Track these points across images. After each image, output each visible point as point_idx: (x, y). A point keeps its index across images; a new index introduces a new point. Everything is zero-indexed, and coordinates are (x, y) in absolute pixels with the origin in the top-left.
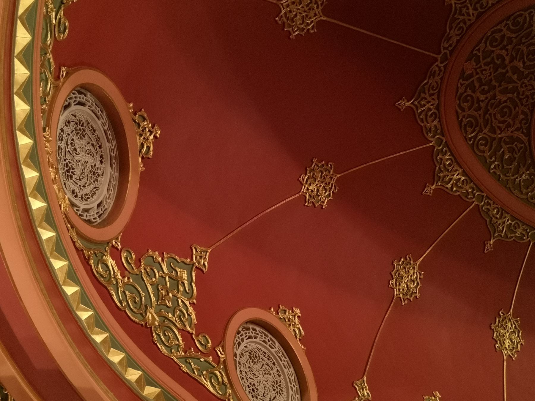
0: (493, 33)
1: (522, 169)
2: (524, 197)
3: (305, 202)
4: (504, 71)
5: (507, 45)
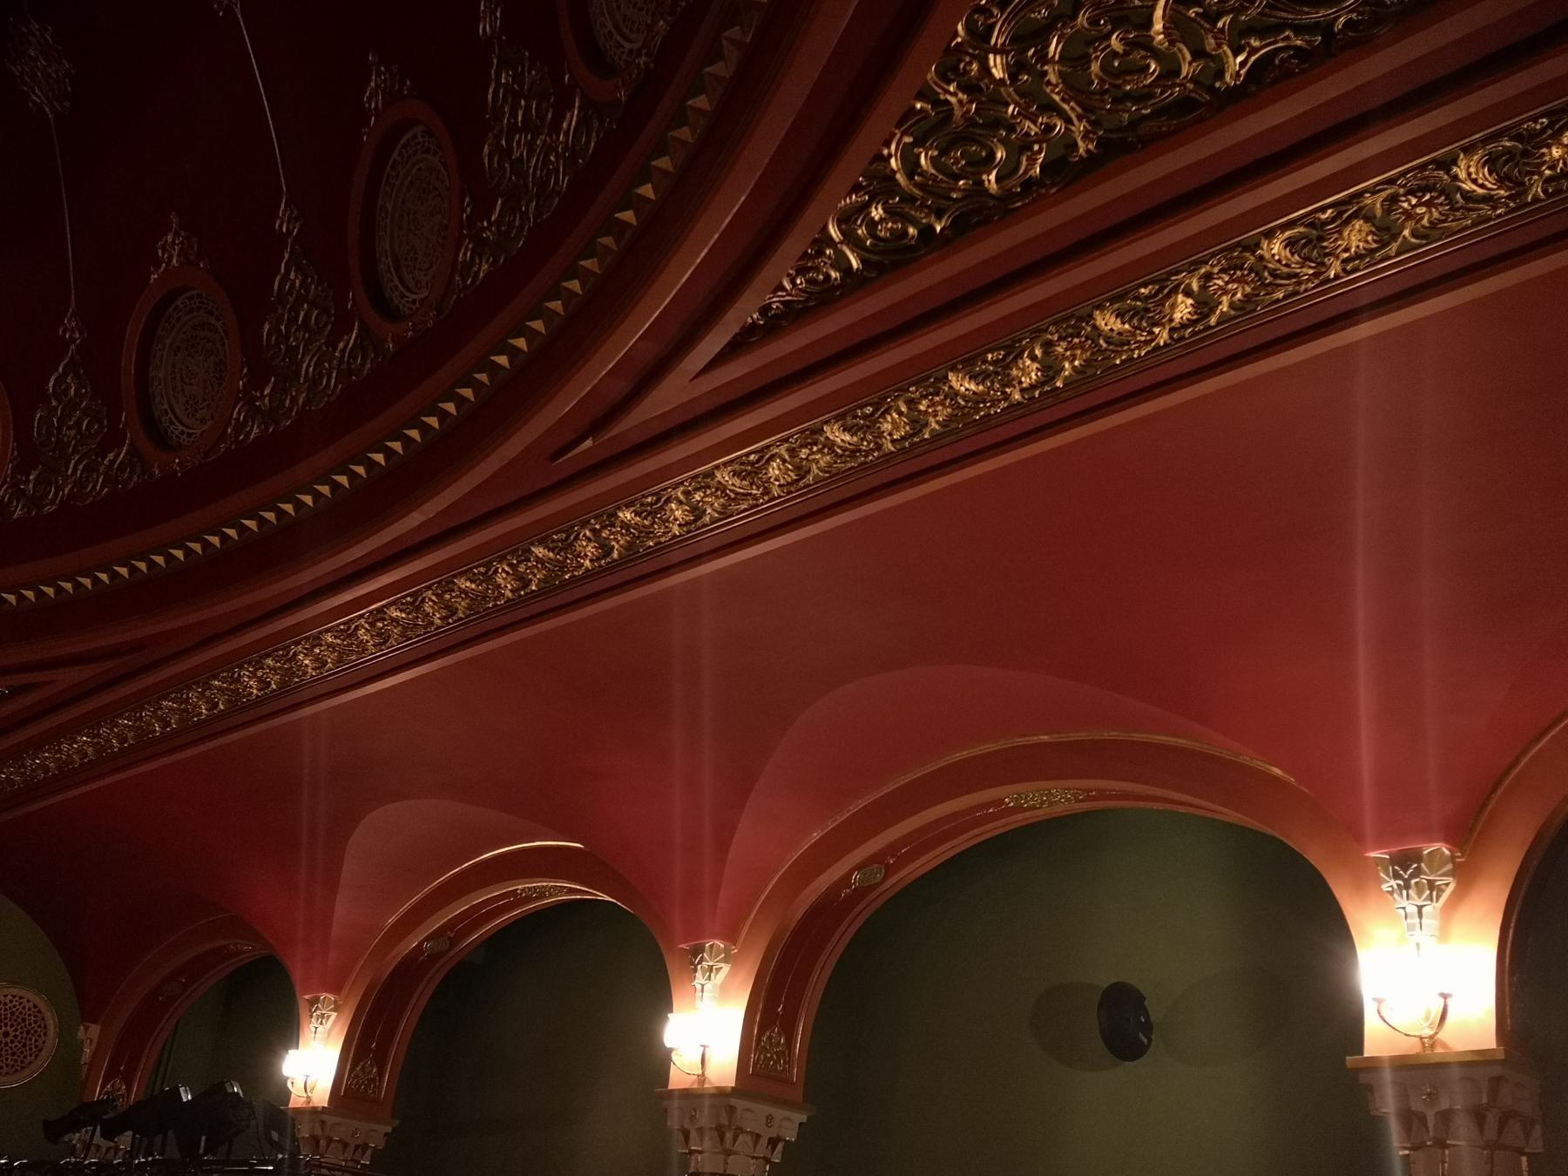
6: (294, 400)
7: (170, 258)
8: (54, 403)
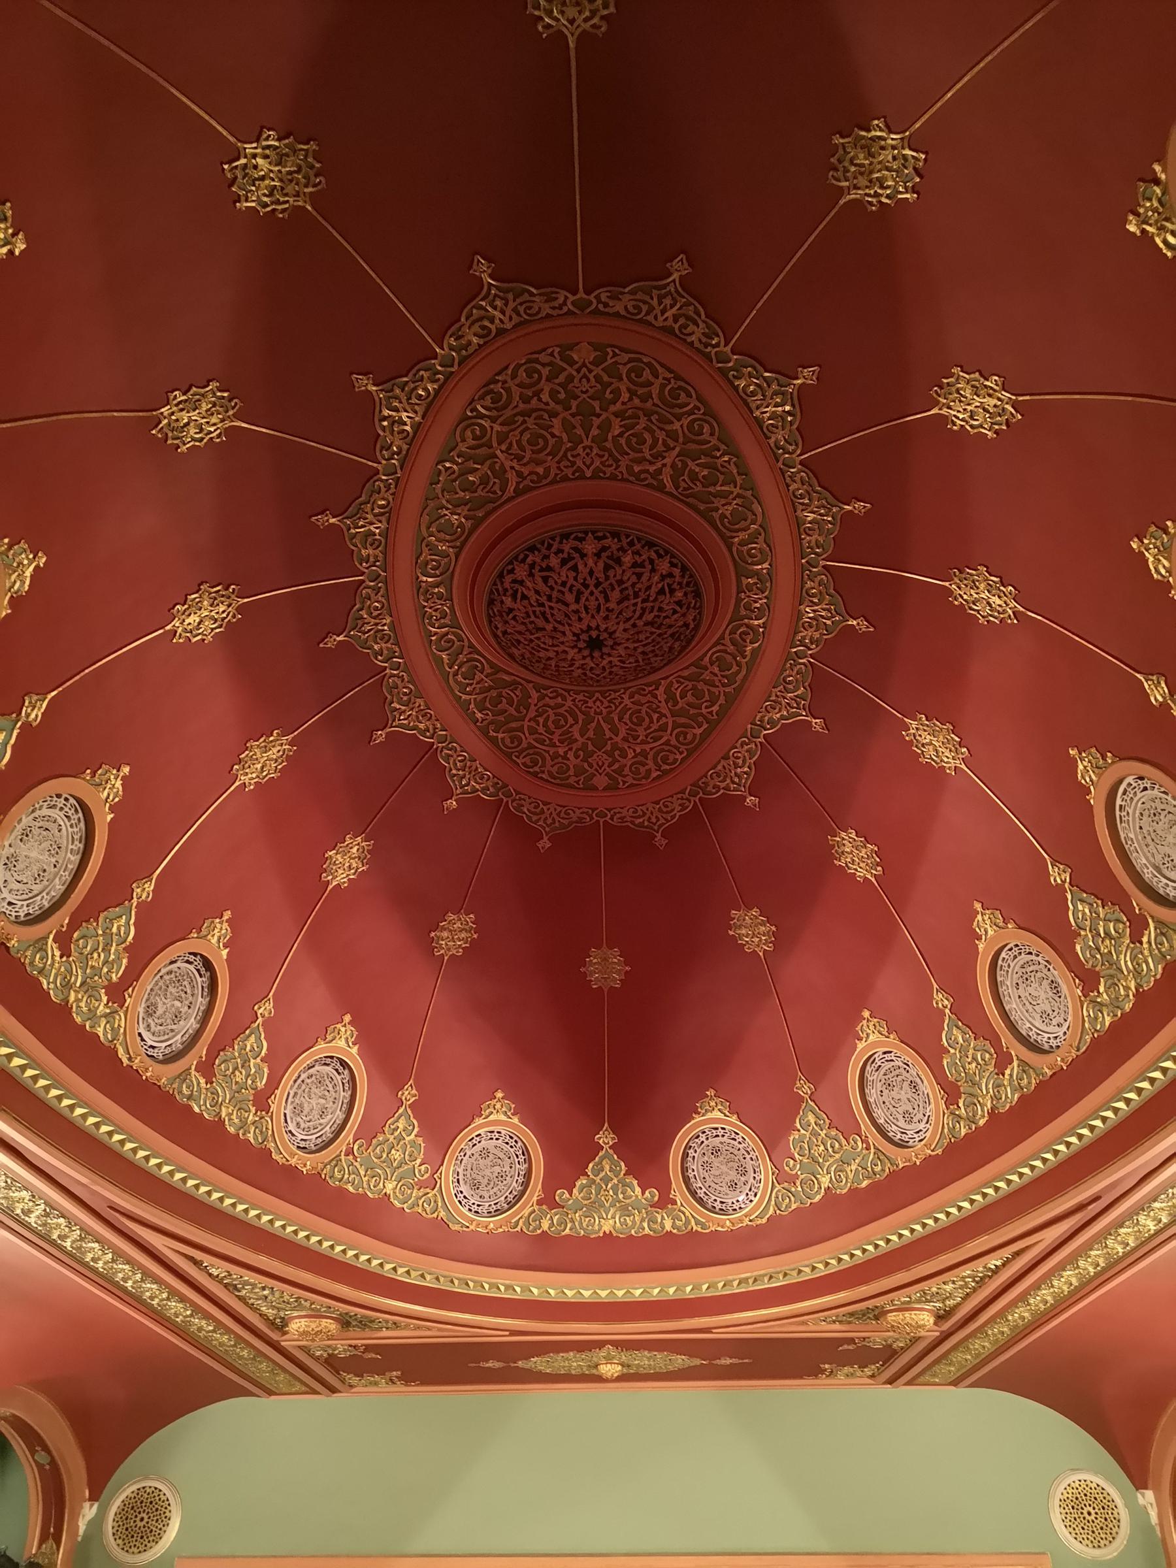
0: (649, 365)
1: (464, 510)
2: (426, 535)
3: (230, 162)
4: (598, 409)
5: (636, 395)
6: (1127, 988)
7: (986, 932)
8: (952, 1051)
